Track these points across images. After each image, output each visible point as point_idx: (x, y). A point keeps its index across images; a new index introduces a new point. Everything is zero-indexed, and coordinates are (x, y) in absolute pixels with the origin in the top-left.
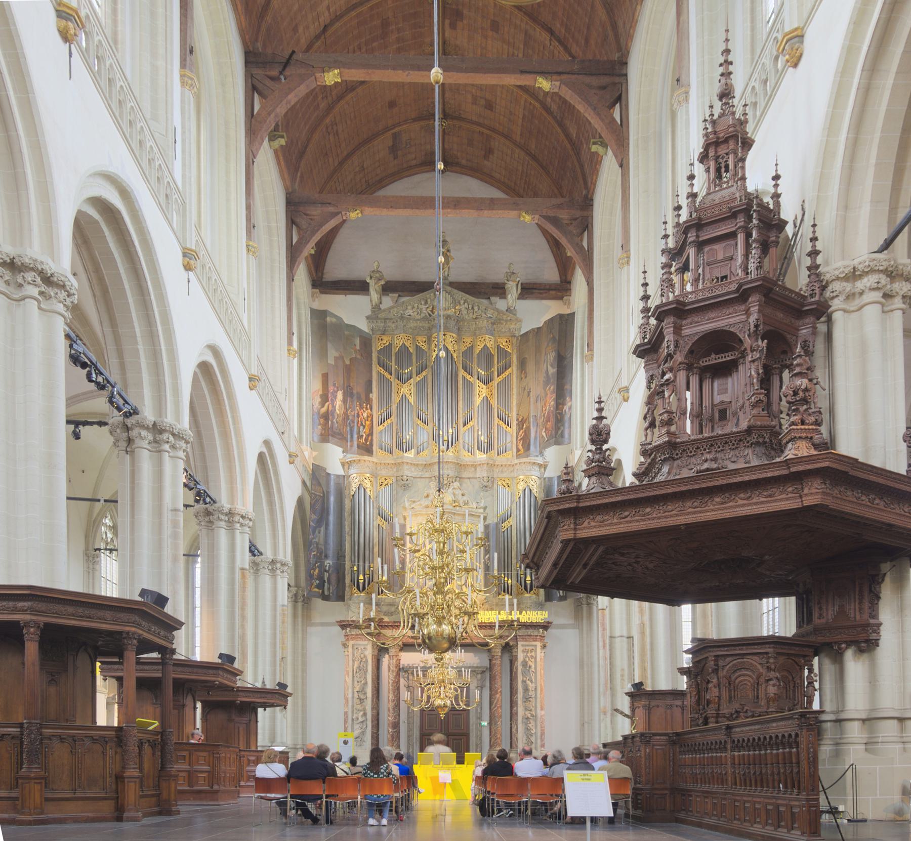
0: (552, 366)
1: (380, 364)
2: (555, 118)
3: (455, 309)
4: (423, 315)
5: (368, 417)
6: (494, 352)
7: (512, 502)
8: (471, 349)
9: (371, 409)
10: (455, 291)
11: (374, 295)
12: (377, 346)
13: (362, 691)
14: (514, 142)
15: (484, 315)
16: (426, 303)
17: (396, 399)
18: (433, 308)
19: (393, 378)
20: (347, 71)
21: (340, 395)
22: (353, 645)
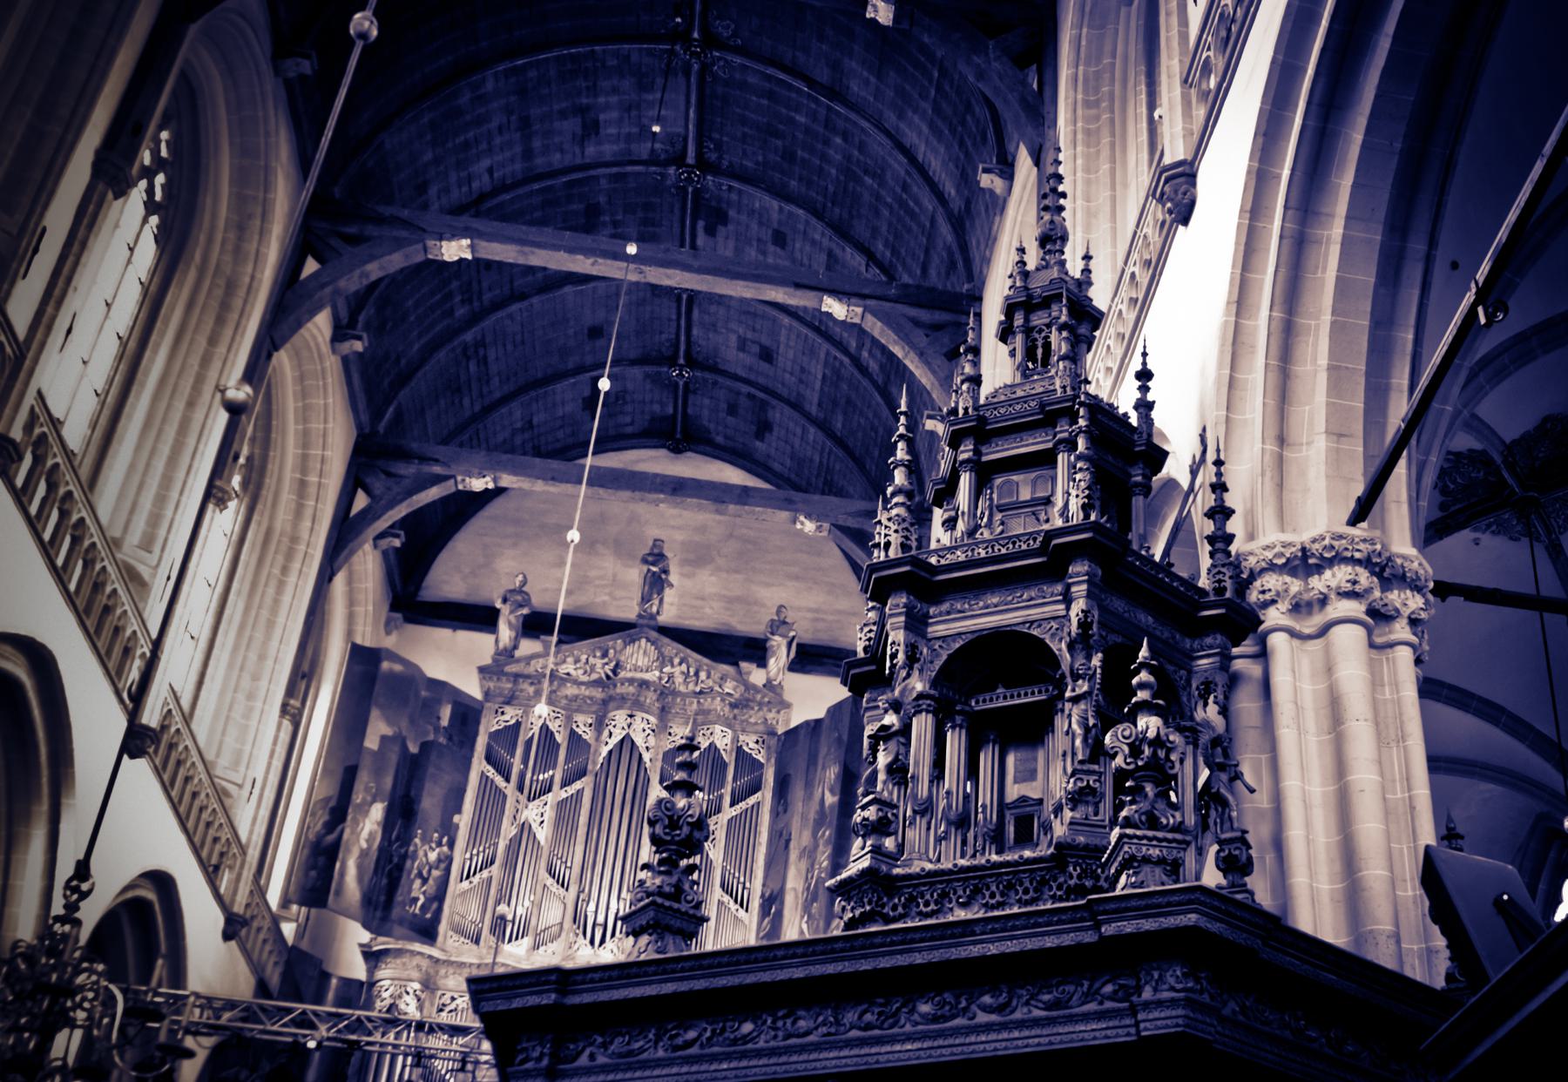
0: (832, 791)
1: (490, 758)
2: (874, 383)
3: (661, 672)
4: (594, 676)
5: (439, 860)
9: (451, 845)
10: (666, 640)
11: (505, 633)
12: (490, 724)
14: (807, 416)
15: (717, 688)
16: (605, 655)
17: (508, 830)
18: (617, 665)
19: (510, 789)
20: (484, 244)
21: (377, 811)
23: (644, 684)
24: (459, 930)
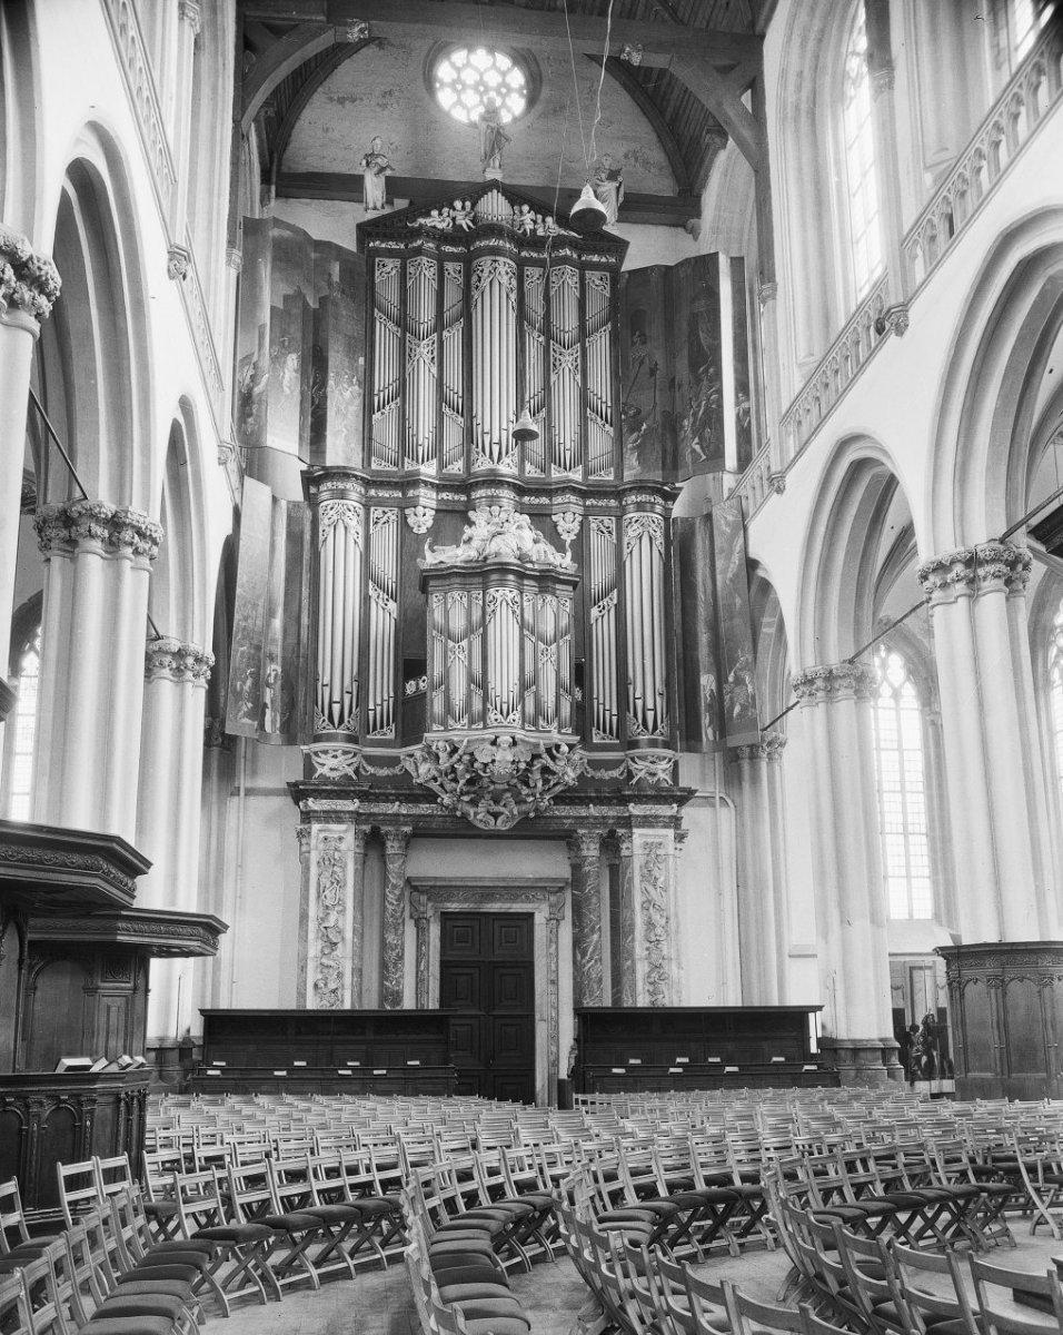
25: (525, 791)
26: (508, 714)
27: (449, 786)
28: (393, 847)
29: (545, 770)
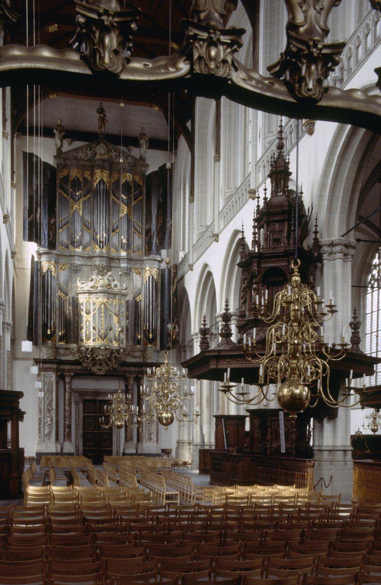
3: (109, 155)
4: (88, 157)
6: (132, 185)
7: (142, 284)
8: (118, 182)
12: (60, 176)
13: (50, 404)
19: (69, 198)
22: (44, 375)
23: (104, 160)
24: (62, 245)
25: (109, 363)
26: (104, 339)
27: (86, 361)
28: (67, 380)
29: (115, 357)
